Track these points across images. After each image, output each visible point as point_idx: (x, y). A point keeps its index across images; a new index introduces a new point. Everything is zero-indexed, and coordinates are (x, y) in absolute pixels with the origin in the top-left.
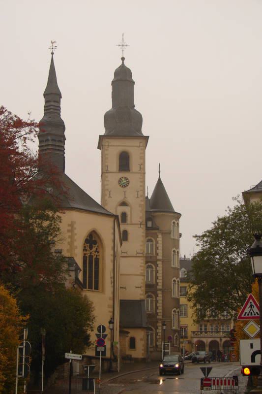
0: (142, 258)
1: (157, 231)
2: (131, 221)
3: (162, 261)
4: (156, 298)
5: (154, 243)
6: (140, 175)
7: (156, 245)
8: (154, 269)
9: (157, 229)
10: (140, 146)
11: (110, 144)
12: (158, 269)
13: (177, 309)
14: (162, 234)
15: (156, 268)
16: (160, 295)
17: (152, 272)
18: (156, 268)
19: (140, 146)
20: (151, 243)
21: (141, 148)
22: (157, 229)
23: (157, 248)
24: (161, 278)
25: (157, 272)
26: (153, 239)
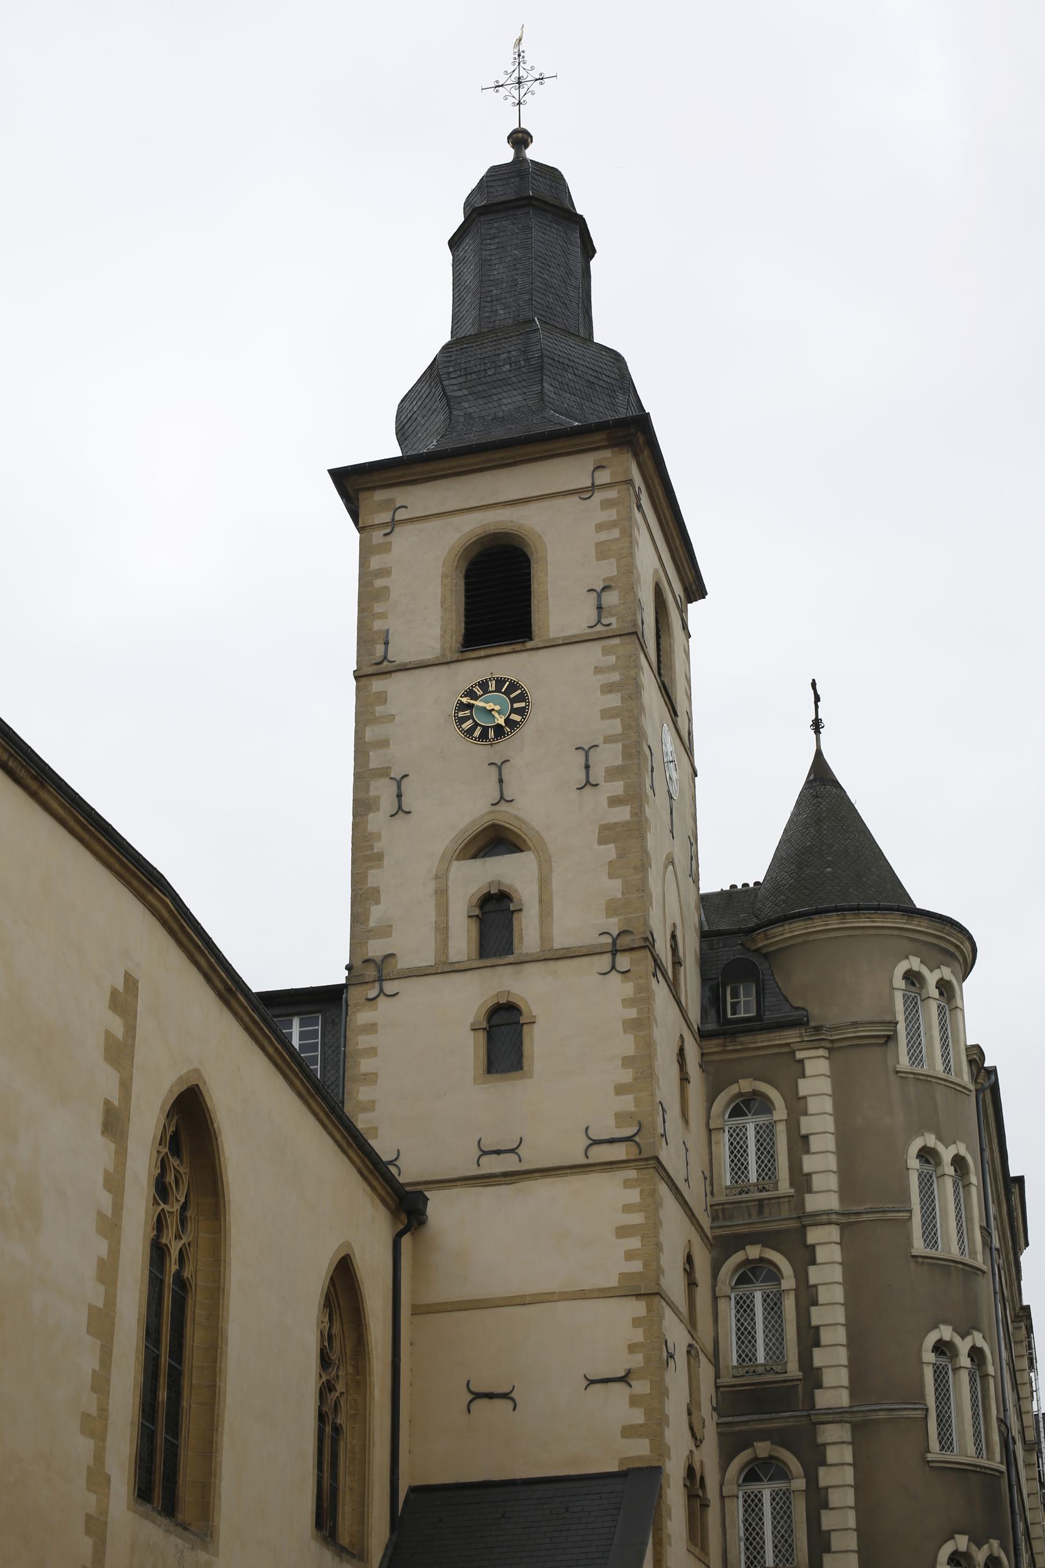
0: (632, 1174)
1: (791, 1036)
2: (545, 936)
3: (843, 1227)
4: (812, 1478)
5: (780, 1113)
6: (596, 648)
7: (793, 1125)
8: (788, 1282)
9: (799, 1022)
10: (593, 488)
11: (401, 515)
12: (815, 1275)
13: (978, 1541)
14: (833, 1050)
15: (802, 1276)
16: (840, 1454)
17: (773, 1306)
18: (802, 1276)
19: (593, 488)
20: (762, 1119)
21: (599, 496)
22: (799, 1022)
23: (800, 1143)
24: (840, 1335)
25: (807, 1296)
26: (773, 1094)
